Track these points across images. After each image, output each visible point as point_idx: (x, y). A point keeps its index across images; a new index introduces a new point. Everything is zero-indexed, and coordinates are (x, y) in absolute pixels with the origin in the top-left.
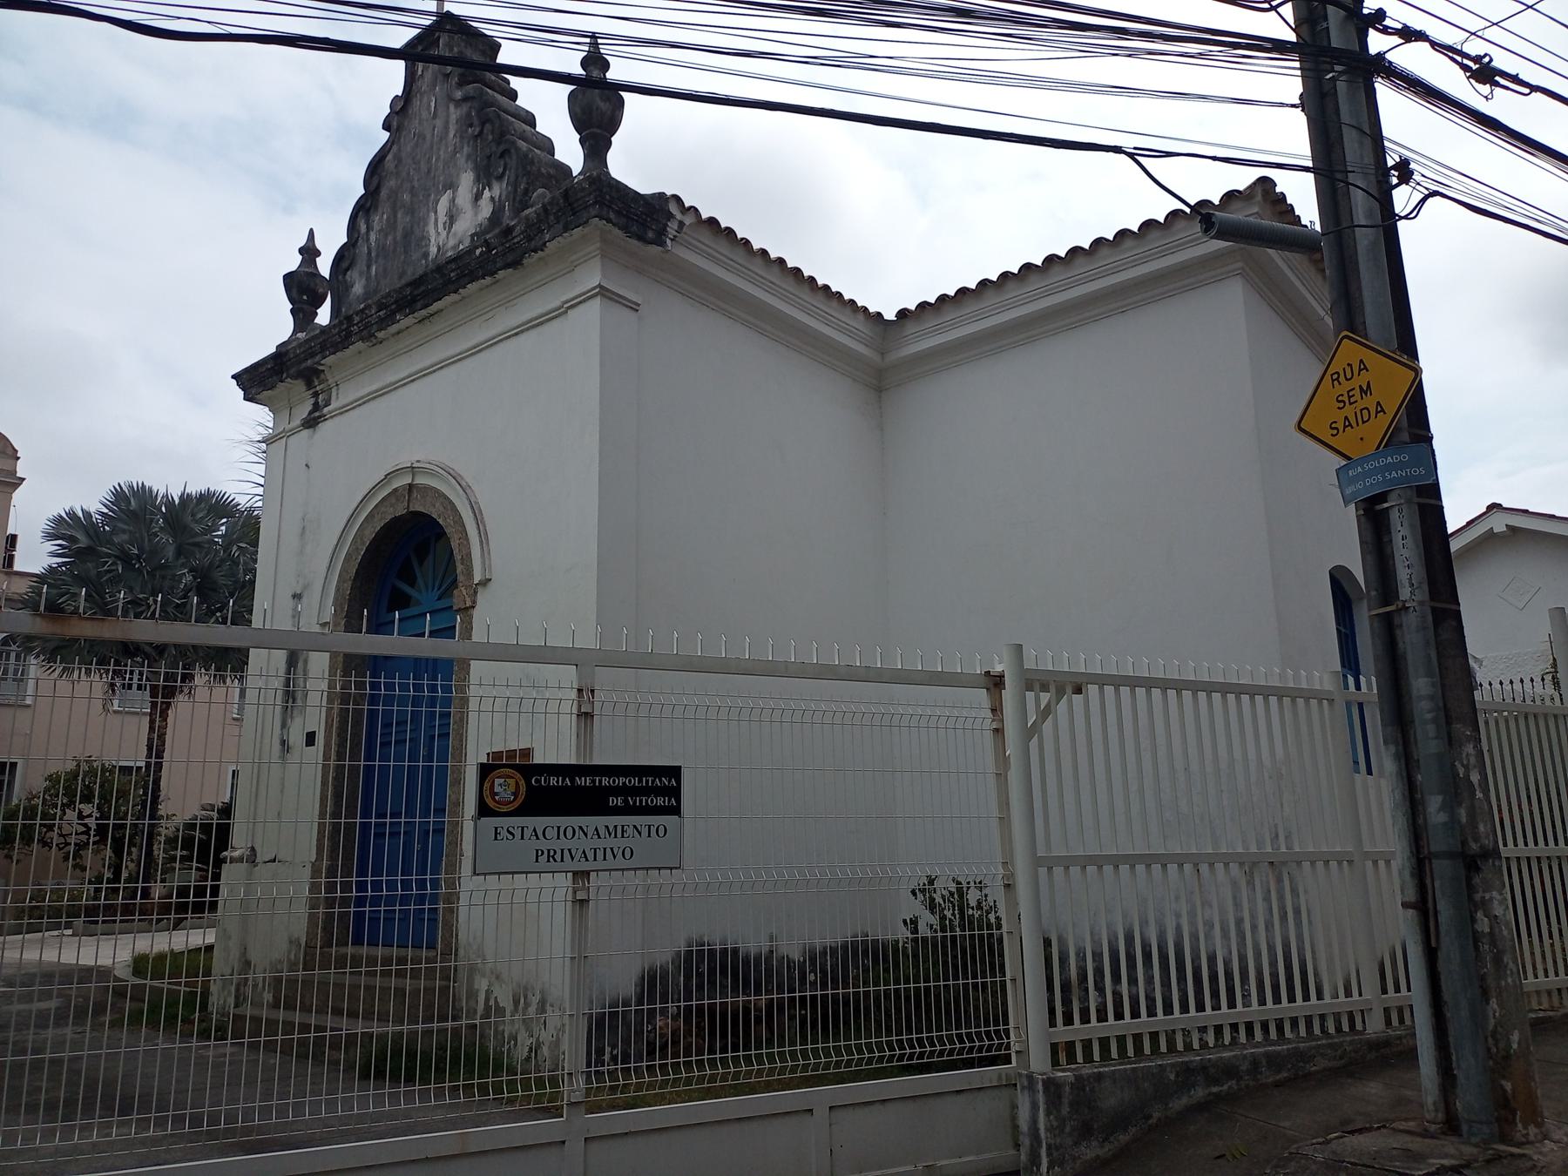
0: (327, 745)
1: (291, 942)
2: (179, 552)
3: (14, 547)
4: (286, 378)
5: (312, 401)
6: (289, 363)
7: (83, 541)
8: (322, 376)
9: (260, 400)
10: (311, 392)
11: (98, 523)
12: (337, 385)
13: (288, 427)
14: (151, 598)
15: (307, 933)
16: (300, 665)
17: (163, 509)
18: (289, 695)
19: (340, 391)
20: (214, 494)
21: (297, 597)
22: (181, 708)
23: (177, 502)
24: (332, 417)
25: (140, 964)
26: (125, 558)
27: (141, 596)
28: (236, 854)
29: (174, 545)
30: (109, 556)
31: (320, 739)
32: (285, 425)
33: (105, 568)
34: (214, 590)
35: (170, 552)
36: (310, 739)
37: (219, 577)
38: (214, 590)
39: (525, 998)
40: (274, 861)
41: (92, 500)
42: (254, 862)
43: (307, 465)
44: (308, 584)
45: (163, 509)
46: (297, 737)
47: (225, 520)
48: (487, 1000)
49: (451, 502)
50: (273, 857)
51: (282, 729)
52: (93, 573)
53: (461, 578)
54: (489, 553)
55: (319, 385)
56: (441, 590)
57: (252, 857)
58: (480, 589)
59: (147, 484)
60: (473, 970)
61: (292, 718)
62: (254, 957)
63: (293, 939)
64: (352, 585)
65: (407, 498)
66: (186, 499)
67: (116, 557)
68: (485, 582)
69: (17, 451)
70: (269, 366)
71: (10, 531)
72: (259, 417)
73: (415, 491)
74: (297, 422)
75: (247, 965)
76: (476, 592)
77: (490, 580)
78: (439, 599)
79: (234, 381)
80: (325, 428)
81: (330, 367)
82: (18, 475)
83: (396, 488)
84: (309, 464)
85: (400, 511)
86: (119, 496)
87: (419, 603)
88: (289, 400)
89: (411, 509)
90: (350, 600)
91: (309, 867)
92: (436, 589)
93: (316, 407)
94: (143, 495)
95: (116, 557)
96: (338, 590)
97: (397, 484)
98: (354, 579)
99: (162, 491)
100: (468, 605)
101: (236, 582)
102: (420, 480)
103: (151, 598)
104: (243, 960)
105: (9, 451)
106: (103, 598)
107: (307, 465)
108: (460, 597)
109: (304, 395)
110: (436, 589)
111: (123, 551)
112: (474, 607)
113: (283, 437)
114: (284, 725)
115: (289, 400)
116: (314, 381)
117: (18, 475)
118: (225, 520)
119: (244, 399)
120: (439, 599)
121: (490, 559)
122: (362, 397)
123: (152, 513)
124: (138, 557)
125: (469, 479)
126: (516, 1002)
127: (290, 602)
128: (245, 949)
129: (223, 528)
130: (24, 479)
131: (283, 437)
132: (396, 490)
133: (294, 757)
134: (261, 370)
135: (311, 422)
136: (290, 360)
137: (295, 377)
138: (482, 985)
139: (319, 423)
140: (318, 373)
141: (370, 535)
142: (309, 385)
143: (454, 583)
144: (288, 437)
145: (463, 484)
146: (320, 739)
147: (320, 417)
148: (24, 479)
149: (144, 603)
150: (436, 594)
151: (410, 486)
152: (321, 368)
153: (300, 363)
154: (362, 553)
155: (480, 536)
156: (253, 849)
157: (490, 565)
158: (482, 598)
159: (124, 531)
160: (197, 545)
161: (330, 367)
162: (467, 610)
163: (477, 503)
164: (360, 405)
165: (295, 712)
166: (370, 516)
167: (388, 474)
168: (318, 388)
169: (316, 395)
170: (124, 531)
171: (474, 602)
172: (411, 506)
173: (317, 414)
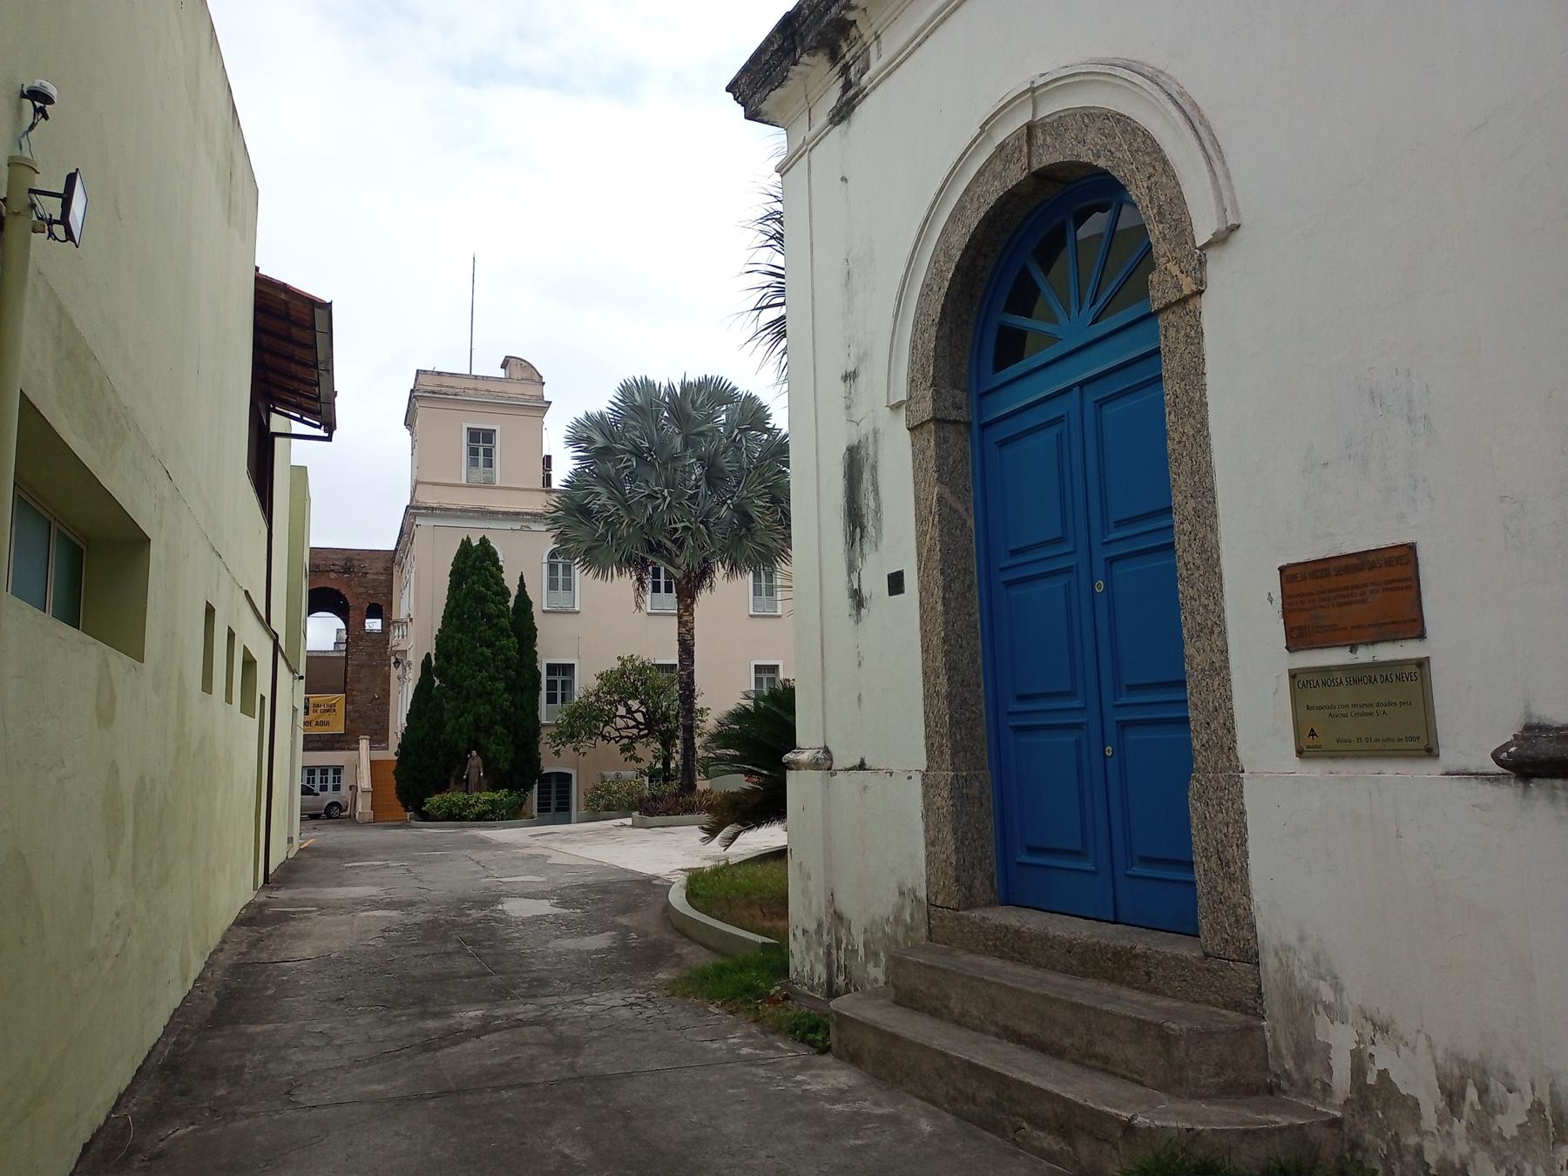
0: (924, 589)
1: (902, 894)
2: (687, 444)
3: (550, 467)
4: (800, 57)
5: (841, 82)
6: (803, 28)
7: (600, 441)
8: (853, 32)
9: (767, 114)
10: (837, 68)
11: (611, 422)
12: (877, 38)
13: (809, 135)
14: (666, 491)
15: (928, 881)
16: (866, 476)
17: (667, 400)
18: (855, 518)
19: (883, 45)
20: (712, 380)
21: (850, 377)
22: (704, 601)
23: (678, 392)
24: (874, 88)
25: (700, 885)
26: (638, 452)
27: (656, 488)
28: (804, 757)
29: (681, 436)
30: (623, 452)
31: (911, 582)
32: (803, 132)
33: (622, 465)
34: (723, 479)
35: (678, 441)
36: (896, 583)
37: (725, 462)
38: (723, 479)
39: (1483, 1091)
40: (862, 766)
41: (602, 400)
42: (830, 769)
43: (844, 179)
44: (865, 354)
45: (667, 400)
46: (874, 584)
47: (724, 408)
48: (1358, 1070)
49: (1120, 119)
50: (858, 762)
51: (849, 577)
52: (613, 471)
53: (1160, 249)
54: (1228, 178)
55: (849, 50)
56: (1098, 305)
57: (824, 762)
58: (1211, 254)
59: (650, 378)
60: (1302, 1006)
61: (863, 555)
62: (849, 907)
63: (905, 889)
64: (937, 331)
65: (1025, 149)
66: (686, 387)
67: (629, 452)
68: (1223, 237)
69: (541, 377)
70: (776, 47)
71: (545, 452)
72: (768, 141)
73: (1039, 134)
74: (822, 119)
75: (838, 917)
76: (1202, 263)
77: (1239, 226)
78: (1094, 322)
79: (730, 95)
80: (865, 111)
81: (865, 9)
82: (545, 399)
83: (1004, 141)
84: (847, 176)
85: (1015, 174)
86: (627, 391)
87: (1054, 340)
88: (806, 98)
89: (1036, 166)
90: (936, 357)
91: (917, 778)
92: (1087, 304)
93: (847, 86)
94: (646, 386)
95: (629, 452)
96: (914, 347)
97: (1001, 136)
98: (940, 323)
99: (665, 384)
100: (1187, 292)
101: (741, 468)
102: (1048, 109)
103: (666, 491)
104: (831, 910)
105: (536, 378)
106: (623, 494)
107: (844, 179)
108: (1161, 288)
109: (827, 78)
110: (1087, 304)
111: (636, 446)
112: (1200, 293)
113: (805, 151)
114: (851, 568)
115: (807, 95)
116: (840, 46)
117: (545, 399)
118: (724, 408)
119: (746, 118)
120: (1094, 322)
121: (1231, 188)
122: (924, 27)
123: (659, 405)
124: (649, 450)
125: (1154, 58)
126: (1452, 1098)
127: (841, 388)
128: (832, 895)
129: (724, 417)
130: (550, 403)
131: (805, 151)
132: (1002, 147)
133: (870, 613)
134: (765, 58)
135: (842, 114)
136: (804, 22)
137: (812, 51)
138: (1340, 1040)
139: (854, 107)
140: (844, 28)
141: (959, 241)
142: (834, 57)
143: (1146, 258)
144: (810, 150)
145: (1146, 70)
146: (911, 582)
147: (856, 95)
148: (550, 403)
149: (659, 496)
150: (1089, 313)
151: (1030, 128)
152: (851, 16)
153: (821, 17)
154: (950, 275)
155: (1204, 149)
156: (826, 750)
157: (1234, 202)
158: (1218, 271)
159: (635, 428)
160: (701, 434)
161: (865, 9)
162: (1186, 302)
163: (1182, 94)
164: (919, 44)
165: (867, 547)
166: (960, 207)
167: (986, 123)
168: (848, 57)
169: (845, 70)
170: (635, 428)
171: (1201, 282)
172: (1034, 161)
173: (852, 92)
